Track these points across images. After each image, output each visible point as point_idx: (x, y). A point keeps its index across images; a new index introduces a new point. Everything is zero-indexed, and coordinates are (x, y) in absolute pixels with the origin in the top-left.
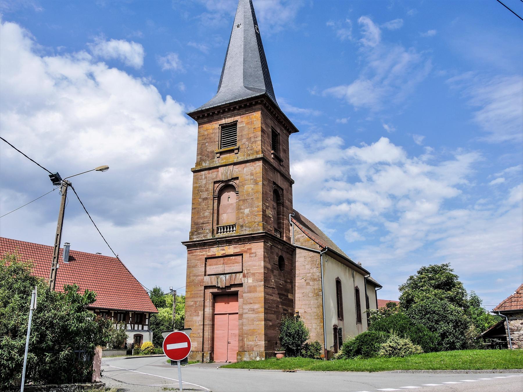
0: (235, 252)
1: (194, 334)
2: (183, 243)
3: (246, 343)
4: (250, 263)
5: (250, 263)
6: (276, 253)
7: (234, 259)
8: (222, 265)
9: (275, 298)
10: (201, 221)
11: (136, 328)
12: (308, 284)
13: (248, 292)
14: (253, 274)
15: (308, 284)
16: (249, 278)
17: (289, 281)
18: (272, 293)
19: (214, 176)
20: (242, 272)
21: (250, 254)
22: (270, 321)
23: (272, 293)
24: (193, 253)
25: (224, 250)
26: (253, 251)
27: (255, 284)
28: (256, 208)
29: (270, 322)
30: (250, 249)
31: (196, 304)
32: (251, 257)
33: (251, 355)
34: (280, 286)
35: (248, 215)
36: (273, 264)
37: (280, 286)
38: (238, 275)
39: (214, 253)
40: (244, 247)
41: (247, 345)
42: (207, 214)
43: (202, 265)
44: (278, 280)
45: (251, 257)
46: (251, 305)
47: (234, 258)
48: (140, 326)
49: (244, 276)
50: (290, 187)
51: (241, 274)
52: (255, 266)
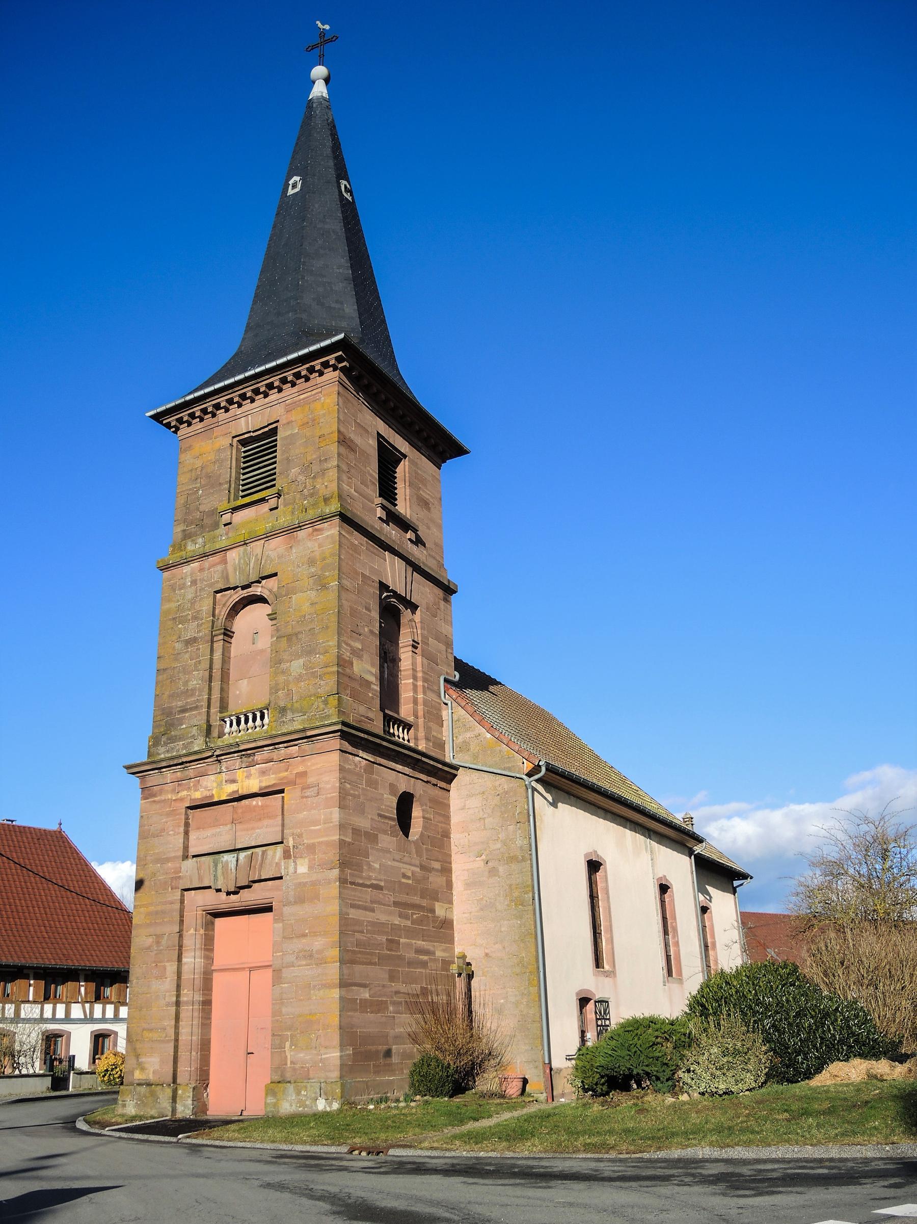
0: (264, 784)
1: (151, 1030)
2: (127, 768)
3: (289, 1057)
4: (301, 816)
5: (301, 816)
6: (387, 785)
7: (262, 806)
8: (229, 826)
9: (383, 918)
10: (180, 704)
11: (98, 1013)
12: (493, 872)
13: (295, 903)
14: (311, 848)
15: (493, 872)
16: (299, 861)
17: (437, 865)
18: (372, 902)
19: (216, 576)
20: (282, 843)
21: (303, 789)
22: (364, 986)
23: (372, 902)
24: (154, 795)
25: (234, 781)
26: (311, 780)
27: (314, 877)
28: (322, 657)
29: (362, 989)
30: (304, 774)
31: (158, 943)
32: (306, 797)
33: (303, 1093)
34: (404, 880)
35: (299, 678)
36: (376, 818)
37: (404, 880)
38: (270, 850)
39: (208, 794)
40: (287, 771)
41: (292, 1062)
42: (195, 682)
43: (177, 830)
44: (396, 864)
45: (306, 797)
46: (304, 940)
47: (260, 804)
48: (110, 1009)
49: (287, 855)
50: (442, 603)
51: (280, 848)
52: (316, 823)
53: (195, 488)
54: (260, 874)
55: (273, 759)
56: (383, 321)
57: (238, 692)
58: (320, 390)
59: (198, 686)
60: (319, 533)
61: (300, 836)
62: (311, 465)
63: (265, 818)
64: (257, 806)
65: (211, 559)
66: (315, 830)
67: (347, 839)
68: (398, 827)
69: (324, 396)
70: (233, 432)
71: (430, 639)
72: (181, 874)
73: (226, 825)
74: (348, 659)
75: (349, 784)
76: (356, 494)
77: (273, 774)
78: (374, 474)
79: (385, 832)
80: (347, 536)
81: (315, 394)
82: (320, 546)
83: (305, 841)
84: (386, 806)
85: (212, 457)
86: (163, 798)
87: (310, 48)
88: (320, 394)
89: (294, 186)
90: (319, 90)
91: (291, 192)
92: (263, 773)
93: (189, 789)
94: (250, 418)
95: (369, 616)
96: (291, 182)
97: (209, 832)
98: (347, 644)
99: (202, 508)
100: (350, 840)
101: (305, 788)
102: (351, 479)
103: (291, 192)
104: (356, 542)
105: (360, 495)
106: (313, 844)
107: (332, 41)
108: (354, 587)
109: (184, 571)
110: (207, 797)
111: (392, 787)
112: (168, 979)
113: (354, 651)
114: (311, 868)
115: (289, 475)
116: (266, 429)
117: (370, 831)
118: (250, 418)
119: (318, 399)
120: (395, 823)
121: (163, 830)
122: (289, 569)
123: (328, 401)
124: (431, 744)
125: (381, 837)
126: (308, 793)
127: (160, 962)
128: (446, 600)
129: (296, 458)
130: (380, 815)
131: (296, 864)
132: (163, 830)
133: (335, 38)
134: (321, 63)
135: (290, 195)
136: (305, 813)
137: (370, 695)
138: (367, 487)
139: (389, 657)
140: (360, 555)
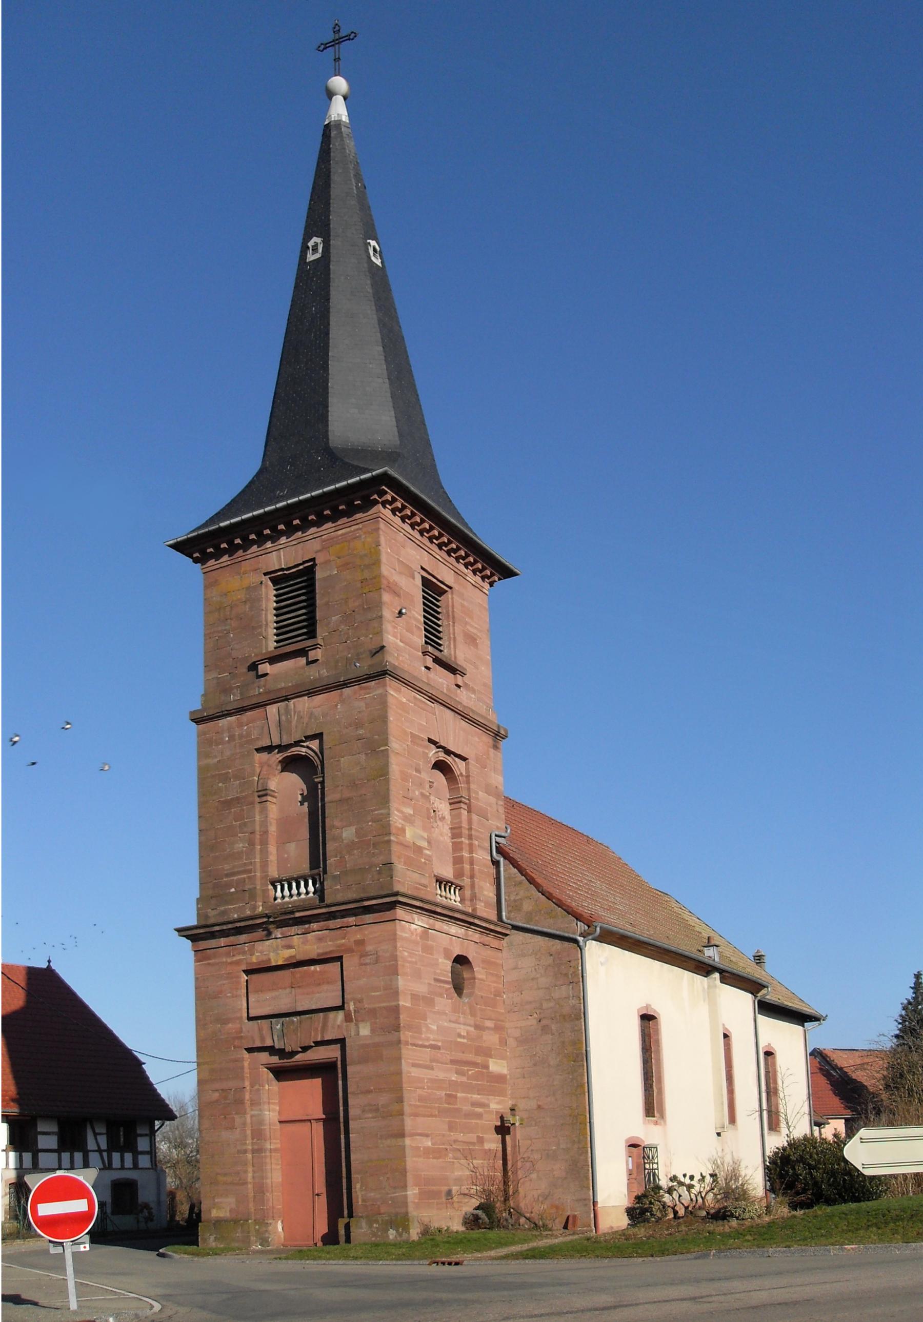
0: (321, 951)
1: (225, 1175)
2: (179, 930)
3: (360, 1196)
4: (363, 981)
5: (363, 981)
6: (442, 950)
7: (320, 972)
8: (288, 990)
9: (441, 1075)
10: (227, 867)
11: (116, 1162)
12: (545, 1029)
13: (359, 1063)
14: (373, 1013)
15: (545, 1029)
16: (361, 1025)
17: (489, 1024)
18: (431, 1061)
19: (255, 732)
20: (341, 1008)
21: (361, 956)
22: (427, 1136)
23: (431, 1061)
24: (209, 958)
25: (290, 947)
26: (369, 948)
27: (377, 1039)
28: (374, 824)
29: (424, 1139)
30: (360, 943)
31: (226, 1098)
32: (365, 964)
33: (375, 1225)
34: (459, 1040)
35: (351, 846)
36: (432, 982)
37: (459, 1040)
38: (332, 1015)
39: (265, 958)
40: (344, 938)
41: (363, 1201)
42: (241, 845)
43: (235, 992)
44: (453, 1025)
45: (365, 964)
46: (370, 1096)
47: (318, 969)
48: (128, 1157)
49: (348, 1018)
50: (492, 750)
51: (341, 1015)
52: (375, 989)
53: (225, 630)
54: (323, 1036)
55: (329, 926)
56: (423, 423)
57: (286, 856)
58: (360, 526)
59: (244, 849)
60: (368, 691)
61: (361, 1001)
62: (354, 613)
63: (323, 983)
64: (315, 971)
65: (249, 713)
66: (374, 996)
67: (407, 1005)
68: (453, 990)
69: (365, 533)
70: (264, 567)
71: (480, 792)
72: (242, 1035)
73: (285, 988)
74: (400, 826)
75: (407, 952)
76: (401, 644)
77: (330, 941)
78: (419, 617)
79: (441, 996)
80: (396, 695)
81: (355, 530)
82: (367, 706)
83: (366, 1006)
84: (441, 970)
85: (241, 595)
86: (217, 961)
87: (323, 47)
88: (360, 531)
89: (315, 249)
90: (339, 110)
91: (311, 257)
92: (320, 939)
93: (244, 953)
94: (282, 553)
95: (419, 778)
96: (310, 244)
97: (268, 995)
98: (398, 811)
99: (235, 654)
100: (410, 1005)
101: (364, 955)
102: (397, 628)
103: (311, 257)
104: (404, 700)
105: (406, 645)
106: (375, 1009)
107: (349, 39)
108: (405, 750)
109: (220, 725)
110: (263, 961)
111: (447, 952)
112: (238, 1129)
113: (406, 817)
114: (373, 1031)
115: (329, 623)
116: (301, 567)
117: (427, 995)
118: (282, 553)
119: (358, 537)
120: (451, 986)
121: (221, 992)
122: (335, 729)
123: (369, 540)
124: (483, 904)
125: (437, 1000)
126: (367, 960)
127: (228, 1115)
128: (496, 747)
129: (337, 604)
130: (436, 980)
131: (358, 1028)
132: (221, 992)
133: (353, 35)
134: (337, 74)
135: (310, 262)
136: (365, 979)
137: (423, 860)
138: (412, 633)
139: (439, 815)
140: (409, 714)
